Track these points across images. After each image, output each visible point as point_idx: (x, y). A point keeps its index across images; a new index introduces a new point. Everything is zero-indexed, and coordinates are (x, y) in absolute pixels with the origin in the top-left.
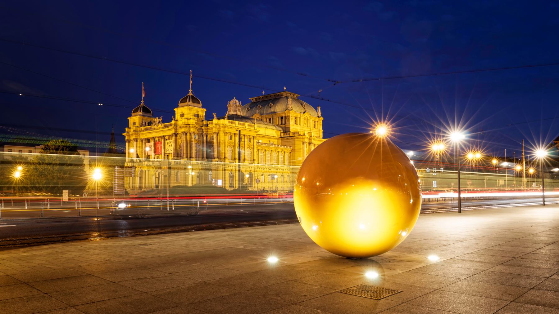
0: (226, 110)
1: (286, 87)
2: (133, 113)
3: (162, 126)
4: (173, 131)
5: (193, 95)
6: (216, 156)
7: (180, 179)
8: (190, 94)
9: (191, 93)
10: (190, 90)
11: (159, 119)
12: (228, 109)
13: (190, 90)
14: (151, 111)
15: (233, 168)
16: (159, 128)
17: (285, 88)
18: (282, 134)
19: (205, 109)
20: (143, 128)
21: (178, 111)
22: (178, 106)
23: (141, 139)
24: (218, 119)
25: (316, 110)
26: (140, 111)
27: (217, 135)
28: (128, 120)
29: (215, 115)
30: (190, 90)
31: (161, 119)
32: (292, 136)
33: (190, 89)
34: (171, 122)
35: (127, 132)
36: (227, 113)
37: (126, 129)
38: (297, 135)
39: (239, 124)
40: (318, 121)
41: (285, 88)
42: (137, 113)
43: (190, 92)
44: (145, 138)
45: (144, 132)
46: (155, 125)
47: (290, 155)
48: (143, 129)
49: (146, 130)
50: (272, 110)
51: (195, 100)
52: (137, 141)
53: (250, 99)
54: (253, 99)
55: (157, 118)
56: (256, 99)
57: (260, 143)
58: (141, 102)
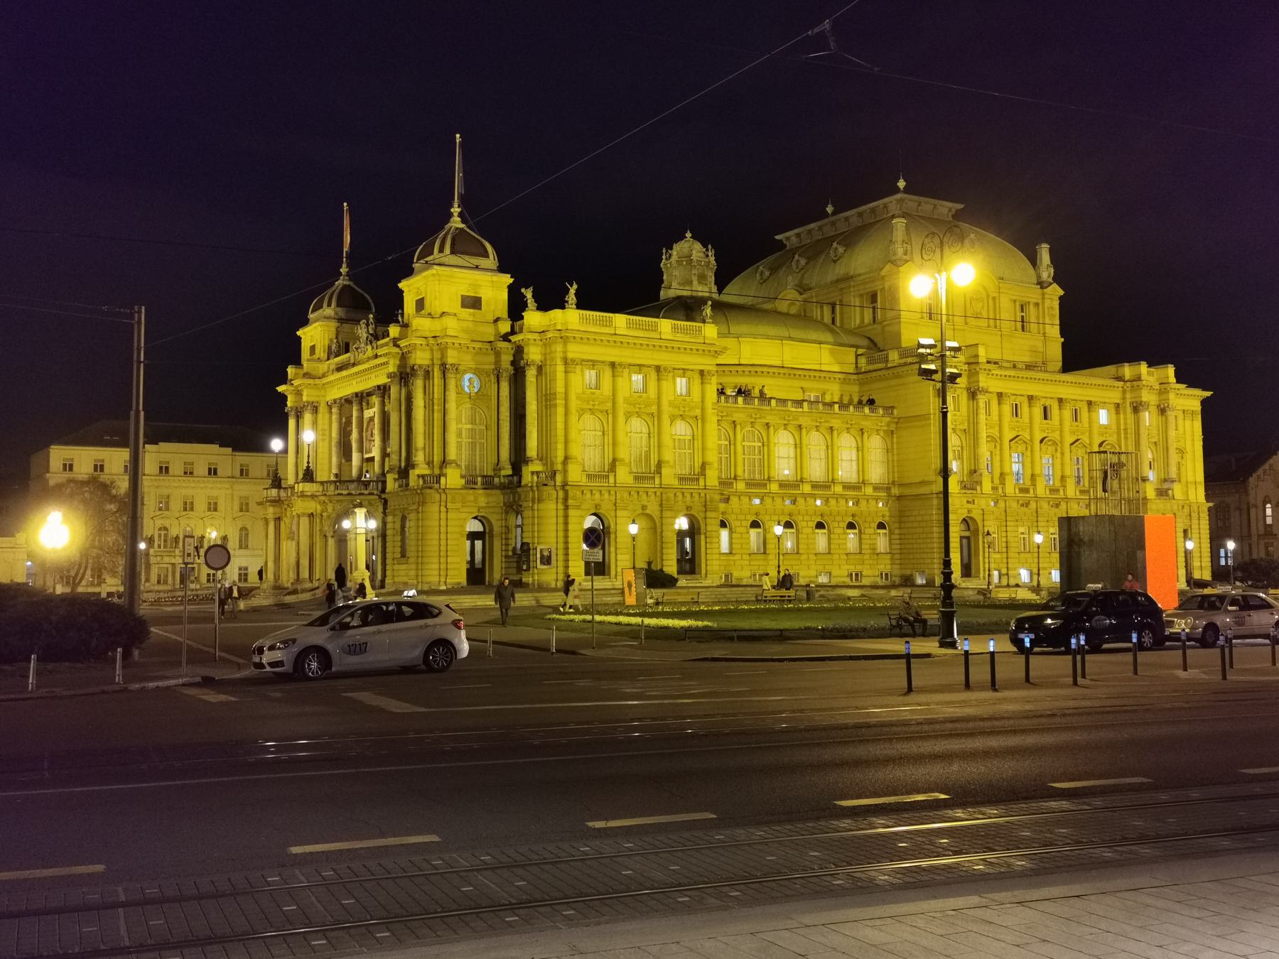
0: (657, 279)
2: (313, 312)
5: (462, 226)
8: (456, 222)
9: (459, 219)
10: (456, 210)
12: (665, 277)
13: (452, 210)
14: (371, 301)
19: (509, 276)
21: (410, 288)
22: (413, 269)
24: (544, 307)
25: (1033, 260)
26: (329, 305)
28: (300, 338)
30: (456, 210)
33: (456, 205)
36: (571, 286)
37: (291, 370)
39: (629, 325)
40: (1040, 301)
42: (321, 311)
43: (456, 214)
44: (341, 399)
46: (359, 350)
47: (892, 443)
50: (840, 270)
51: (461, 246)
53: (777, 237)
54: (788, 239)
56: (798, 235)
57: (773, 402)
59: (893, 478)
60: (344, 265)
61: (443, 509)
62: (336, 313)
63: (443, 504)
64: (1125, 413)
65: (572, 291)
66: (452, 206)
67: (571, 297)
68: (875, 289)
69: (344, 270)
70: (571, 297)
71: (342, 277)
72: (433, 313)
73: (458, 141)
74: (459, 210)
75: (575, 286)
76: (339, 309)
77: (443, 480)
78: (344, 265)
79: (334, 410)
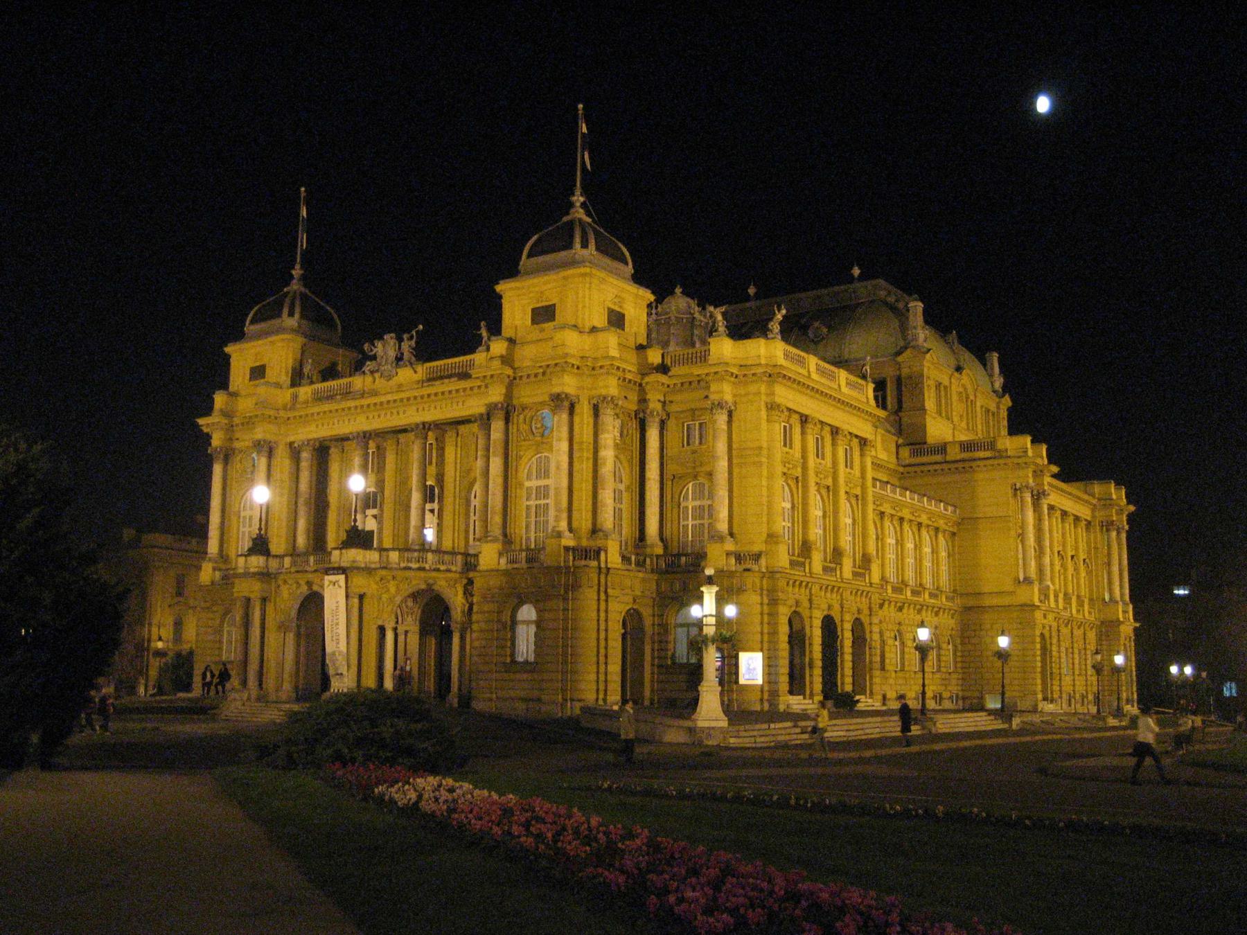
1: (860, 268)
3: (418, 376)
4: (496, 394)
6: (723, 526)
7: (472, 647)
9: (581, 211)
10: (578, 199)
11: (400, 340)
13: (574, 198)
14: (335, 316)
15: (803, 590)
16: (400, 386)
17: (856, 272)
18: (905, 452)
20: (305, 391)
23: (291, 444)
24: (739, 332)
26: (291, 314)
27: (730, 414)
28: (227, 358)
29: (719, 317)
30: (578, 199)
31: (413, 343)
32: (958, 457)
34: (472, 350)
35: (221, 410)
36: (779, 311)
38: (988, 454)
40: (995, 410)
41: (856, 272)
43: (578, 204)
45: (316, 410)
46: (377, 375)
47: (953, 546)
48: (302, 397)
49: (319, 398)
52: (270, 454)
55: (390, 338)
58: (292, 277)
59: (955, 586)
60: (298, 266)
61: (603, 596)
62: (300, 326)
63: (602, 589)
64: (1095, 532)
65: (779, 317)
66: (573, 194)
67: (775, 326)
68: (884, 376)
69: (297, 272)
70: (775, 326)
71: (295, 281)
72: (580, 325)
73: (580, 112)
74: (582, 199)
75: (784, 312)
76: (304, 322)
77: (603, 555)
78: (298, 266)
79: (305, 455)
